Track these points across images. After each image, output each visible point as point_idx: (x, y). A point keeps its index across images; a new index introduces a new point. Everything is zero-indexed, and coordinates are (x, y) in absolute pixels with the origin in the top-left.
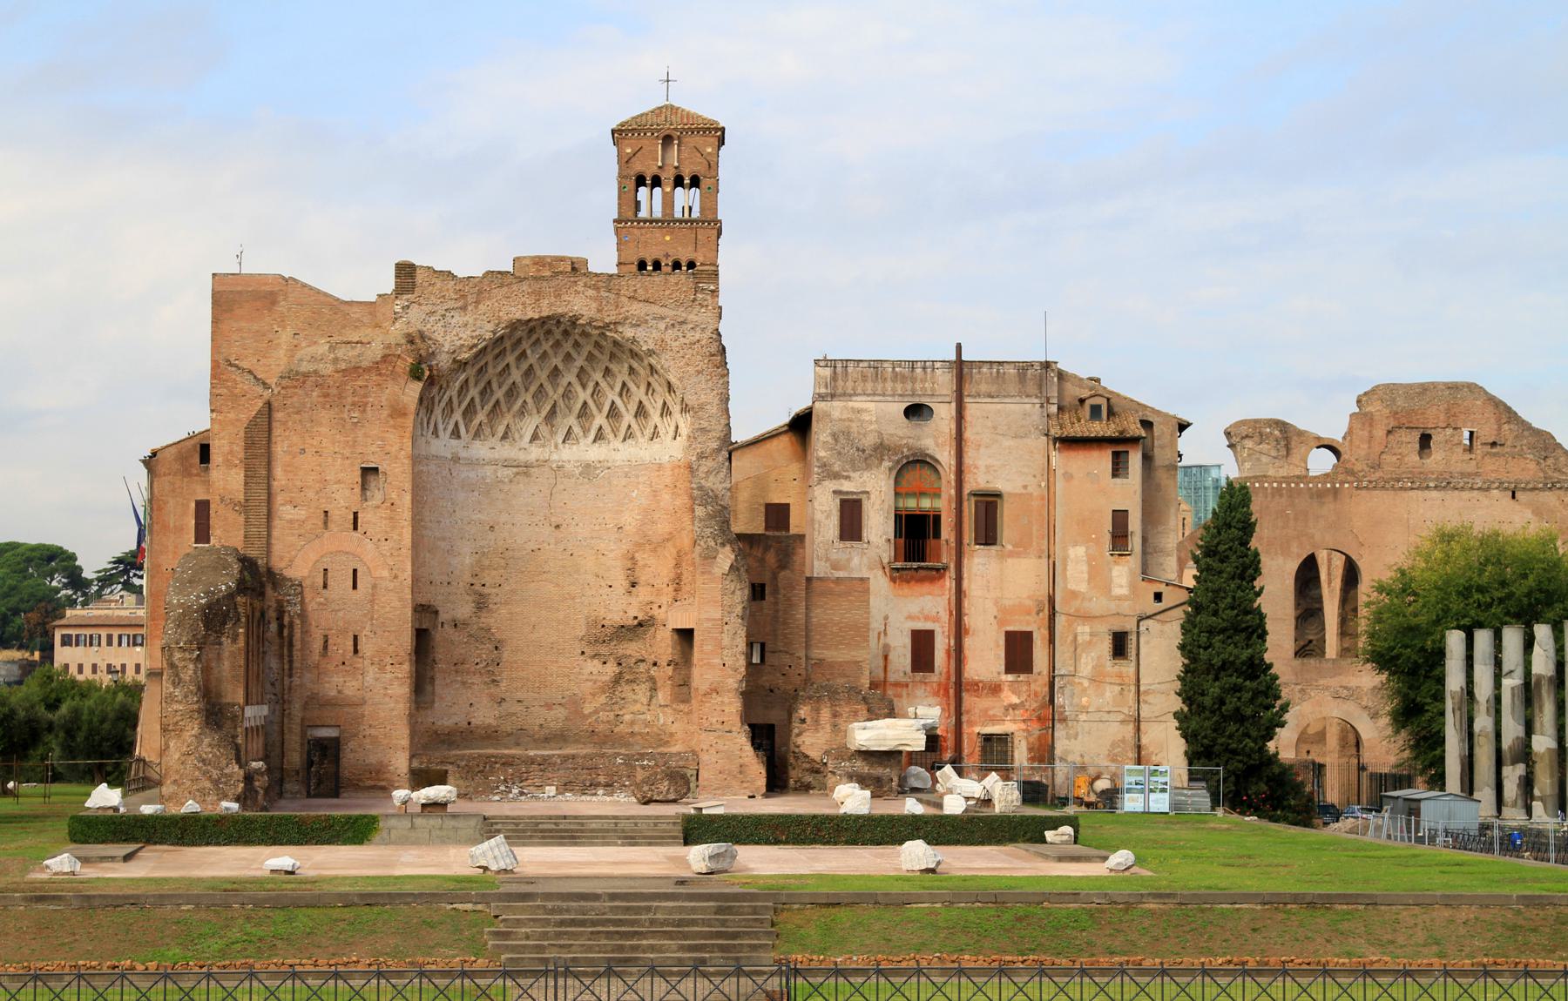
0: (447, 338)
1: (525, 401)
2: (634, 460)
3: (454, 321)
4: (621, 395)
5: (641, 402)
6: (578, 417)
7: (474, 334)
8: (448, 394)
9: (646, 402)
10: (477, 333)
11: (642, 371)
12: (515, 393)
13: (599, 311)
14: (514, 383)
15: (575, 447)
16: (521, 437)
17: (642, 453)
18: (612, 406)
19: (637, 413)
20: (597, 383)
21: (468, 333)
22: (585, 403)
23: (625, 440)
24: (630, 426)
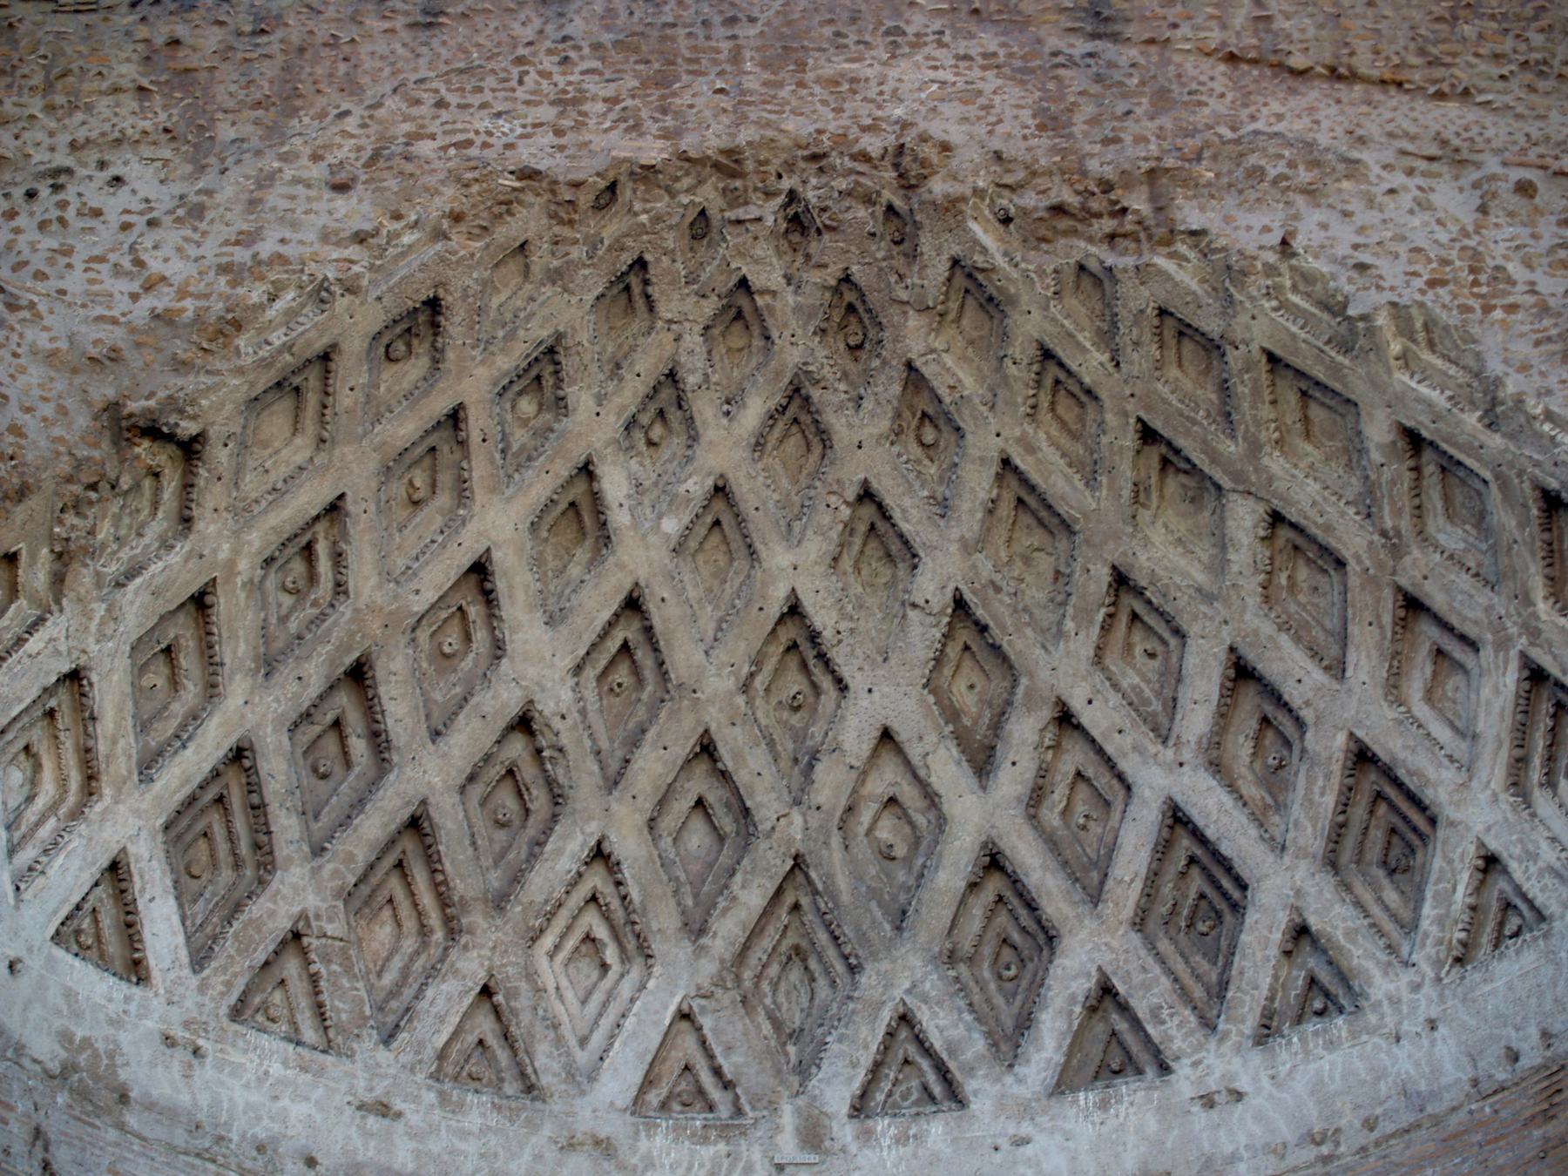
0: (75, 283)
1: (600, 854)
2: (1349, 1120)
3: (115, 204)
4: (1217, 767)
5: (1362, 757)
6: (952, 957)
7: (242, 255)
8: (55, 627)
9: (1391, 745)
10: (266, 248)
11: (1353, 539)
12: (539, 799)
13: (1050, 122)
14: (524, 723)
15: (937, 1130)
16: (582, 1078)
17: (1404, 1062)
18: (1163, 848)
19: (1339, 831)
20: (1065, 719)
21: (210, 248)
22: (994, 862)
23: (1266, 1032)
24: (1301, 932)
